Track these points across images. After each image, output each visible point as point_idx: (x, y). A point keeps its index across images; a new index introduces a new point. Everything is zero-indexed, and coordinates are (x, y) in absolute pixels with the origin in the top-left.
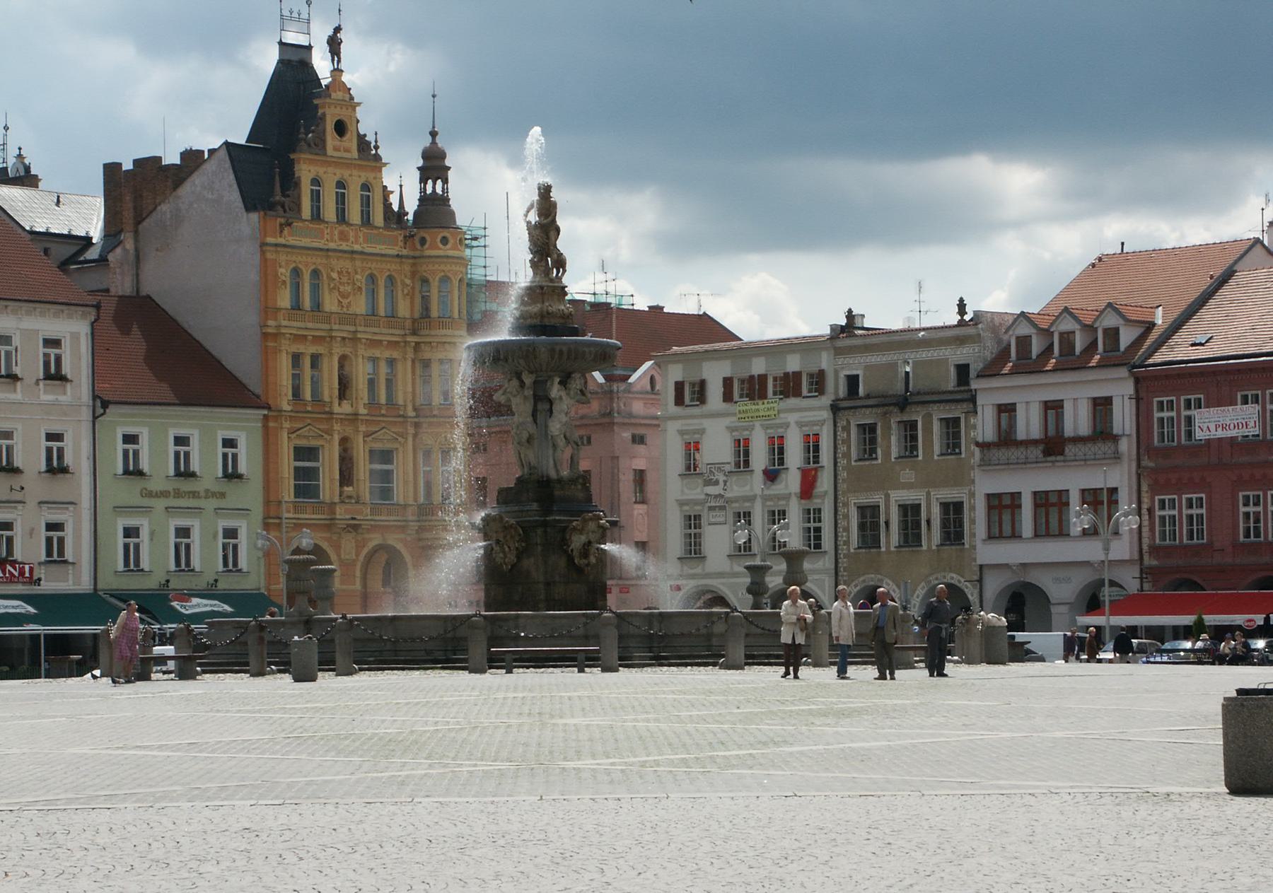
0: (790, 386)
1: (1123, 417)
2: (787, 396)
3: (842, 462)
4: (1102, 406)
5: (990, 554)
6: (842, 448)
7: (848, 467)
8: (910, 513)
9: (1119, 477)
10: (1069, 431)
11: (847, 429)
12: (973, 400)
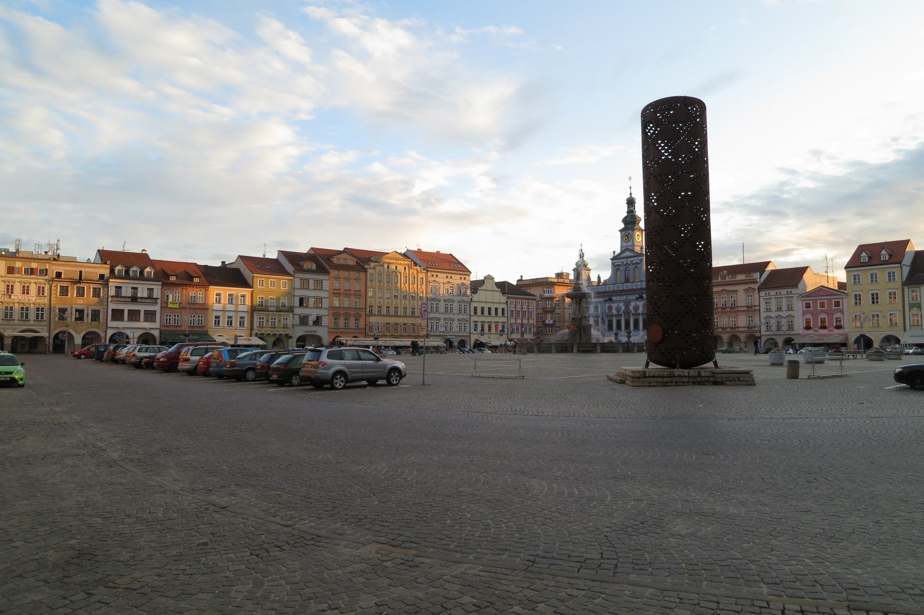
0: (32, 271)
1: (157, 293)
2: (32, 274)
3: (53, 296)
4: (151, 290)
5: (111, 324)
6: (53, 292)
7: (56, 297)
8: (80, 312)
9: (157, 308)
10: (139, 295)
11: (56, 286)
12: (107, 284)
